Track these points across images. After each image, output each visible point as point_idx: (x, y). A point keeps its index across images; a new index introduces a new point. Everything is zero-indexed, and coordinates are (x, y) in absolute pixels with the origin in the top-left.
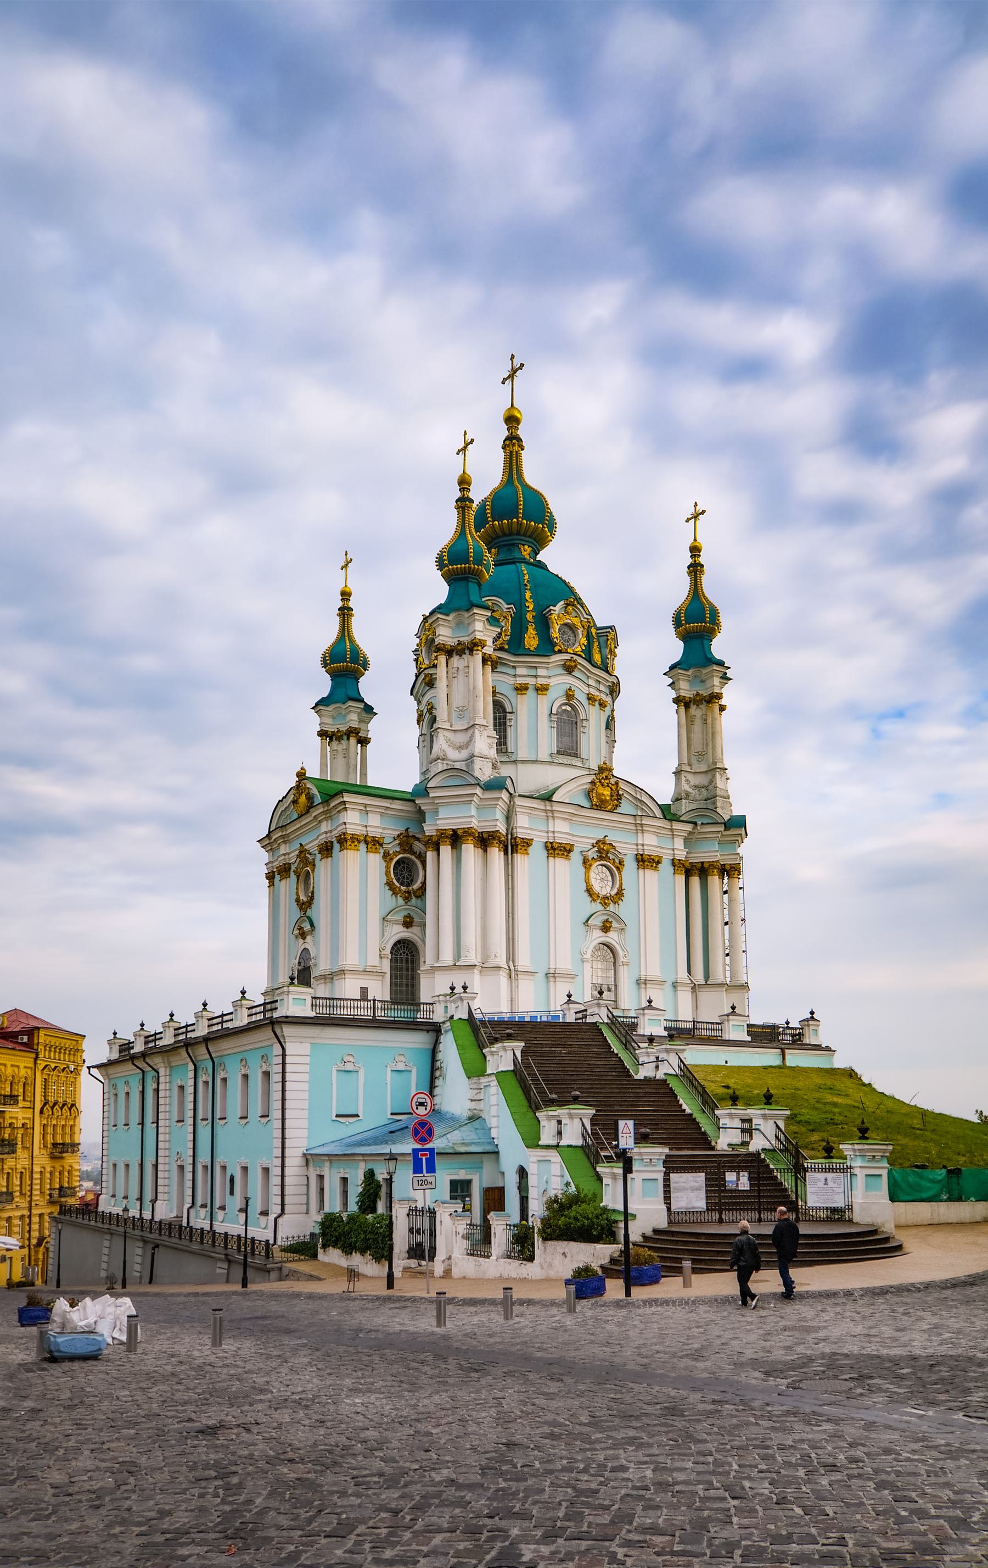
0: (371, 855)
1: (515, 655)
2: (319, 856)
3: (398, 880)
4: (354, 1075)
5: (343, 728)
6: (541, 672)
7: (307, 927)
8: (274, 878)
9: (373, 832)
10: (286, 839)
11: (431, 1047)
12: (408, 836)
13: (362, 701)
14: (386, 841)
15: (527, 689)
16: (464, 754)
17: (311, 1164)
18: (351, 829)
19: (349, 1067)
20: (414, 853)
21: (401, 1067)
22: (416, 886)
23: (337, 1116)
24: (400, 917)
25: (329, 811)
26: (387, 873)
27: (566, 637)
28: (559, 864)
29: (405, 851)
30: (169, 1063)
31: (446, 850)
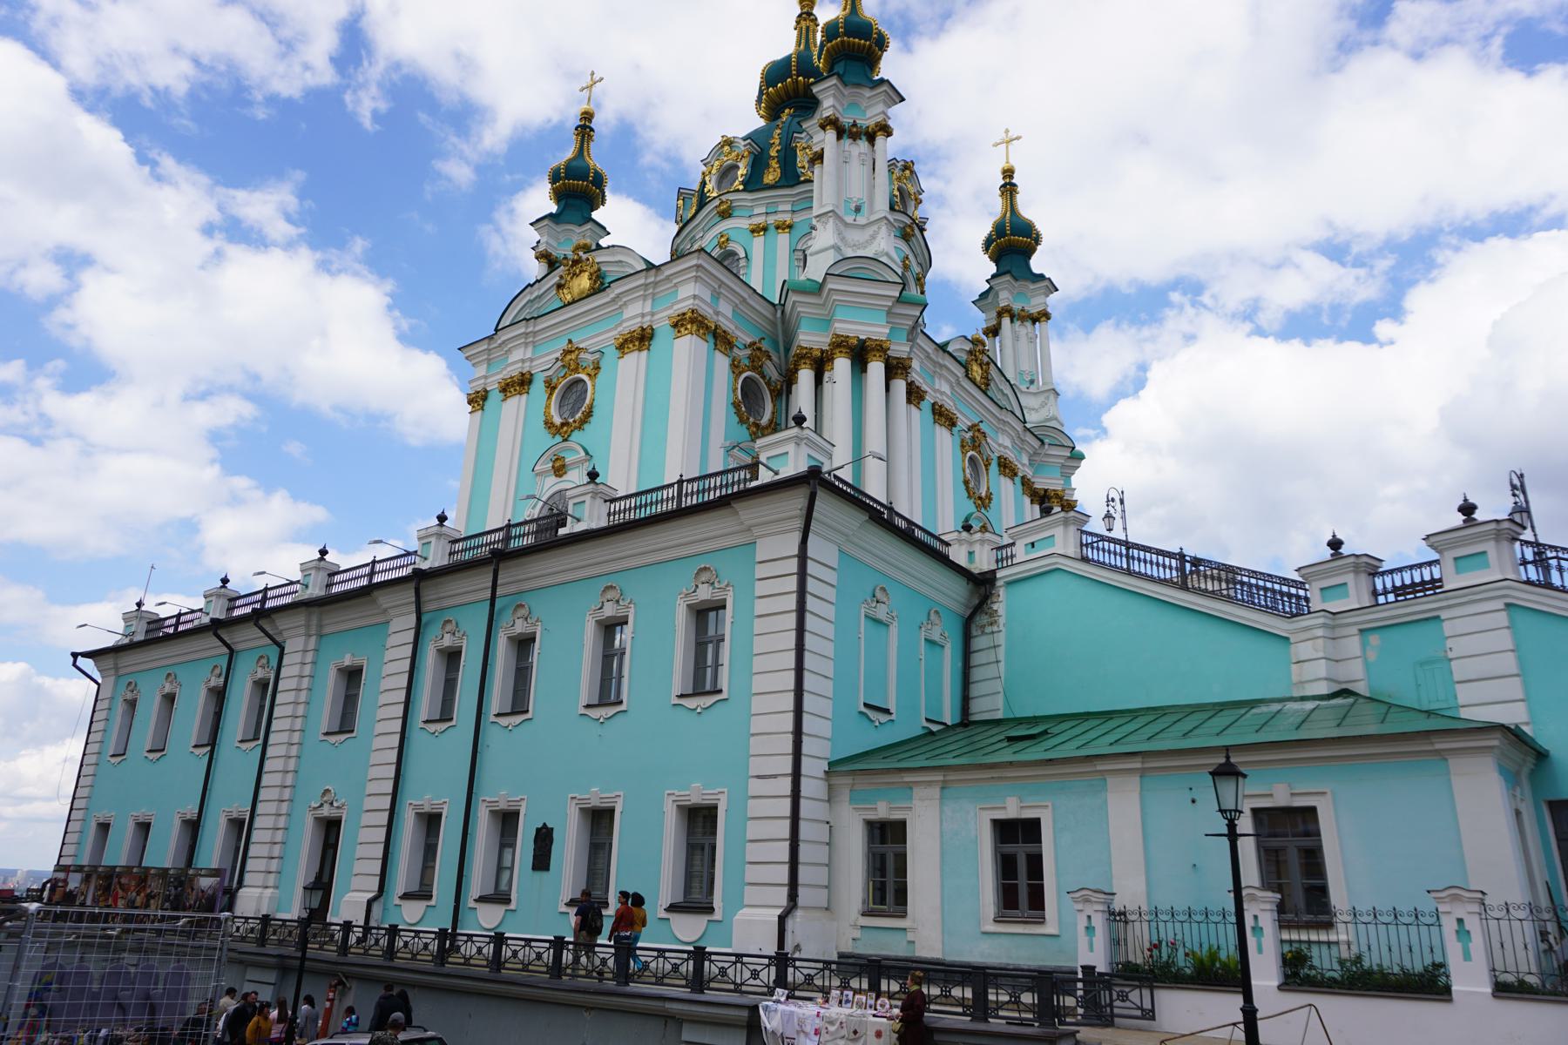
0: (718, 354)
2: (611, 352)
4: (883, 629)
8: (485, 398)
10: (529, 340)
11: (968, 612)
17: (845, 795)
19: (881, 612)
20: (763, 377)
21: (936, 637)
22: (765, 421)
23: (866, 705)
25: (656, 284)
26: (735, 390)
29: (754, 369)
30: (320, 626)
31: (842, 366)
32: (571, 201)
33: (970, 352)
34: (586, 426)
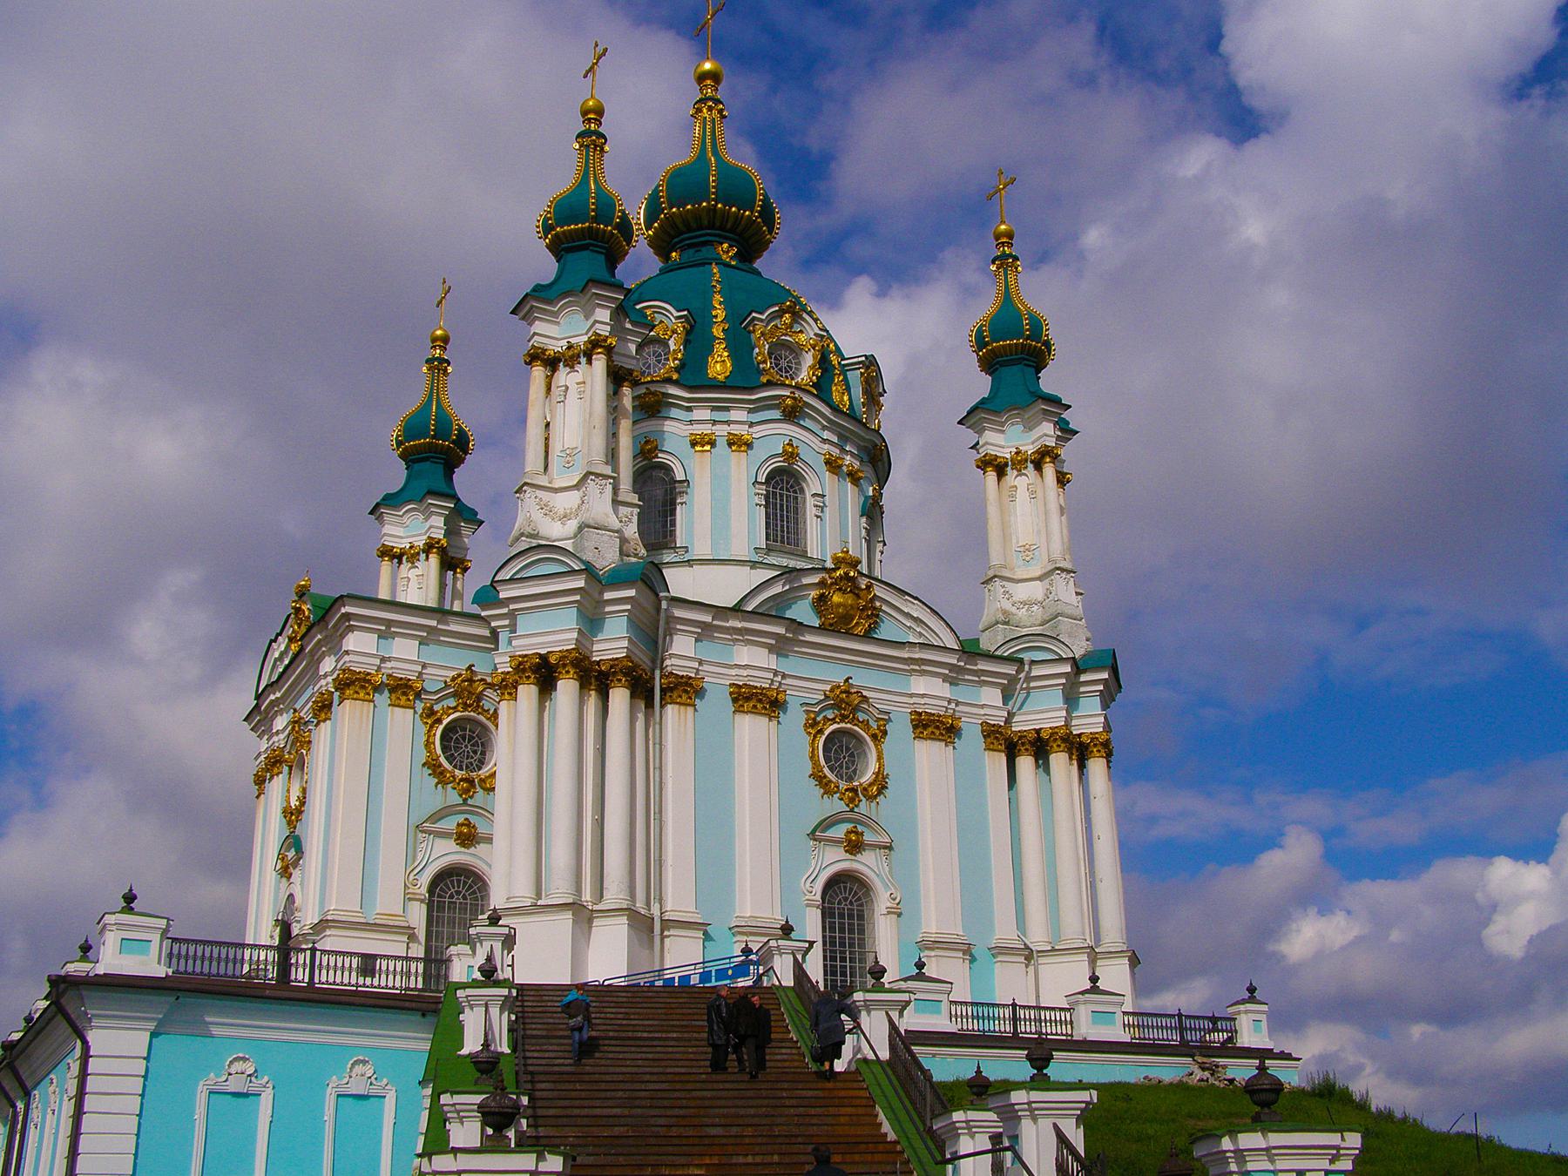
1: (691, 388)
3: (450, 759)
5: (420, 542)
6: (738, 415)
7: (291, 854)
9: (408, 672)
12: (471, 681)
13: (453, 497)
14: (429, 687)
15: (713, 444)
16: (572, 525)
18: (359, 665)
24: (450, 824)
26: (428, 744)
27: (783, 363)
28: (751, 729)
29: (466, 707)
32: (416, 466)
33: (822, 584)
34: (304, 816)
